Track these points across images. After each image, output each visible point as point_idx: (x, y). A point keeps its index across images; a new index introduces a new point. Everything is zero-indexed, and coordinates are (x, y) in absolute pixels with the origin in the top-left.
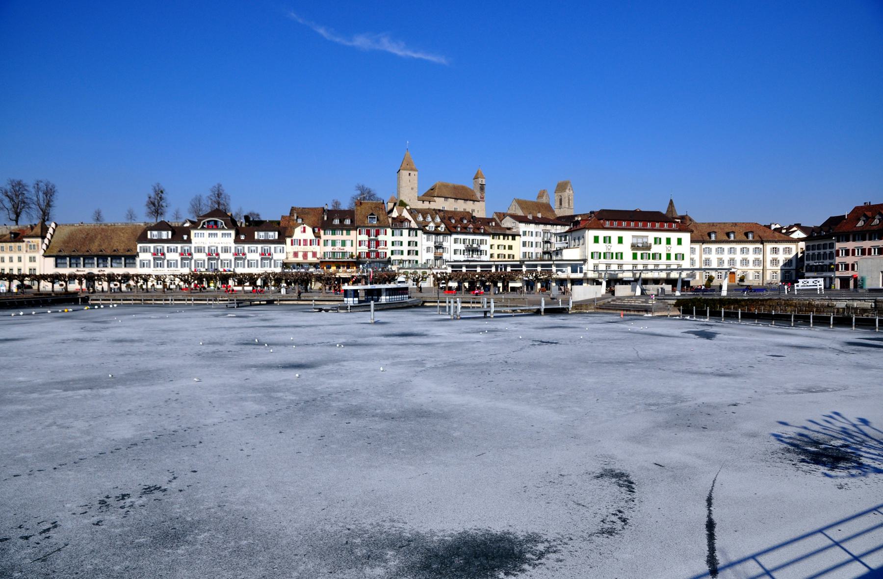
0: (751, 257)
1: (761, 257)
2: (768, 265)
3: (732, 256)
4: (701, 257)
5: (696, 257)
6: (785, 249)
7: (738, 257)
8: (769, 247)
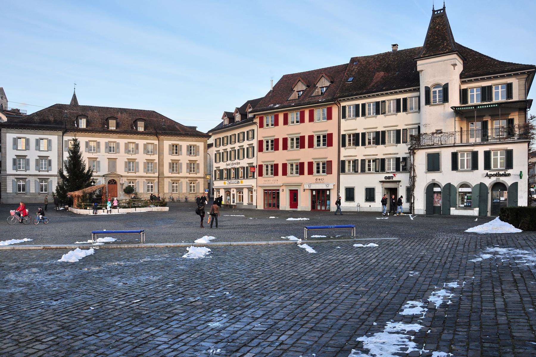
0: (141, 158)
2: (167, 172)
3: (112, 156)
6: (190, 148)
7: (122, 158)
8: (167, 143)
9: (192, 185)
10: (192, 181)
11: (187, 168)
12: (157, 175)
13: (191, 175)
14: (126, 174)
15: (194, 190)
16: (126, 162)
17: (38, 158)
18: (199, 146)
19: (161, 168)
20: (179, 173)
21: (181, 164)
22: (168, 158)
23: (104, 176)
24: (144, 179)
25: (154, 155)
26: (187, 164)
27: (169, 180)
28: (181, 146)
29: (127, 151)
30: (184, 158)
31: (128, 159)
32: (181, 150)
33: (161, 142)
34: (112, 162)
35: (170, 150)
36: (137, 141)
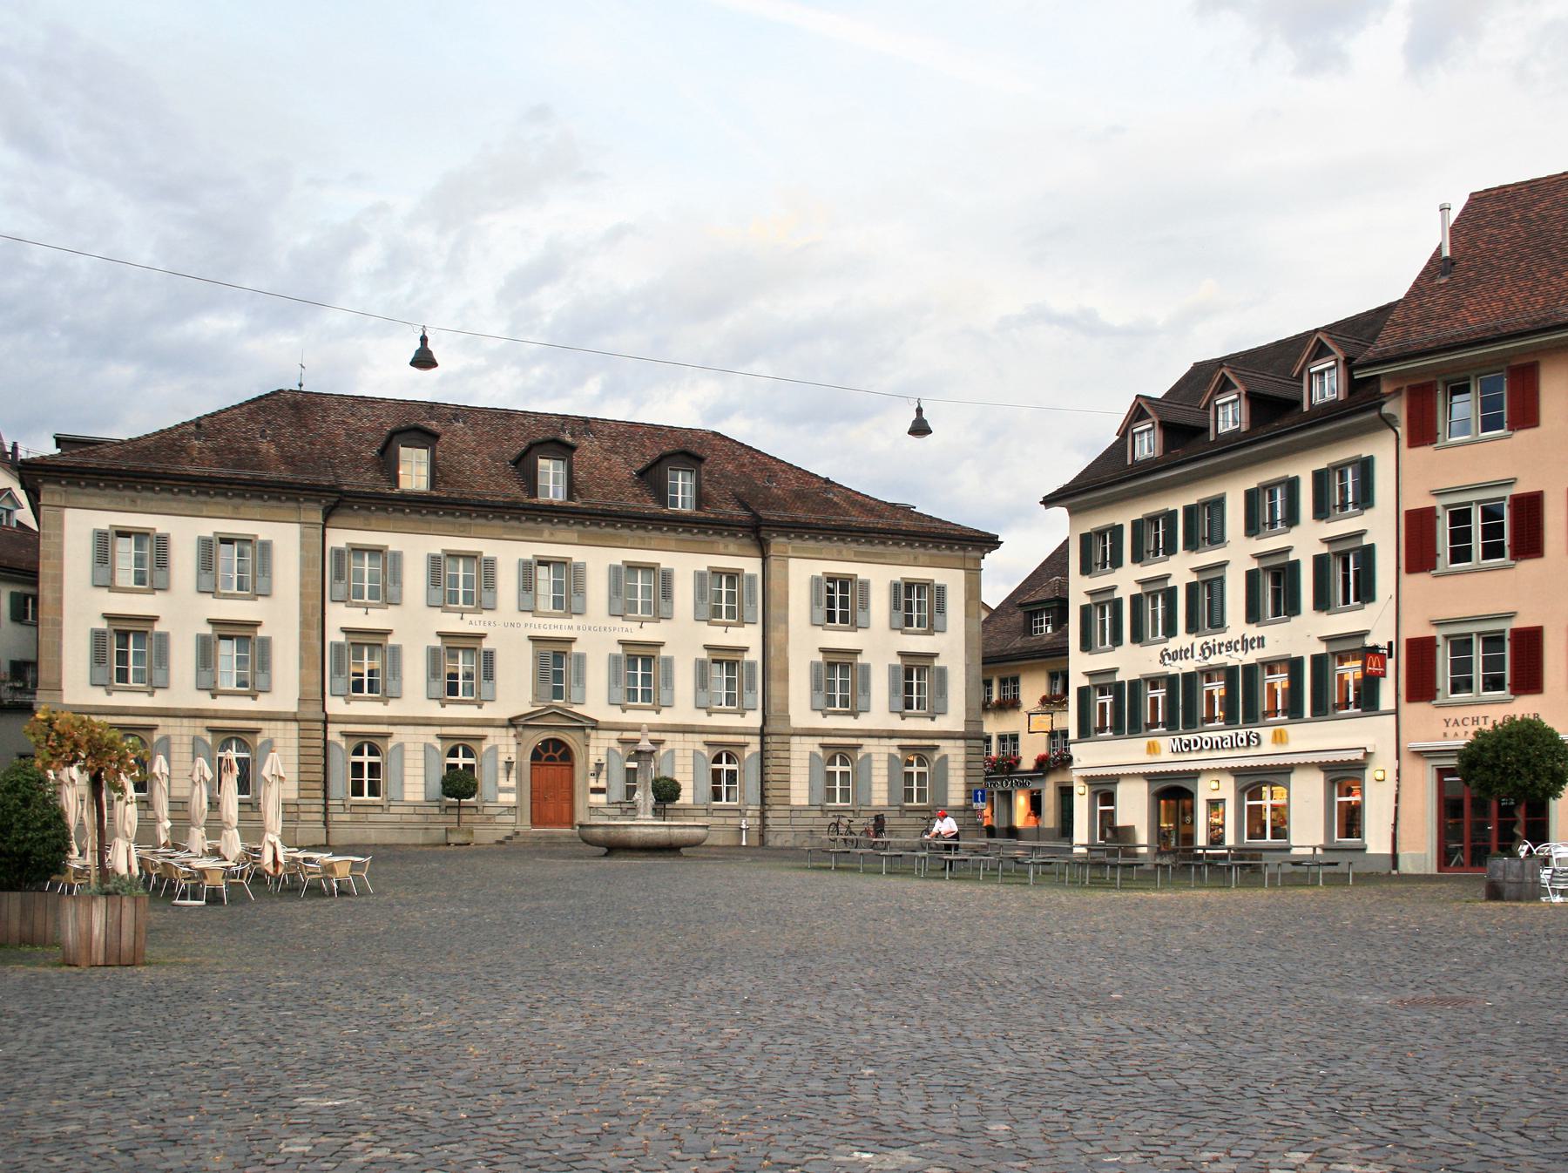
0: (684, 637)
1: (748, 637)
4: (314, 620)
5: (278, 616)
7: (597, 636)
8: (803, 572)
9: (915, 769)
10: (920, 751)
11: (893, 691)
12: (754, 720)
13: (912, 725)
14: (615, 715)
15: (921, 797)
16: (614, 659)
17: (208, 630)
18: (941, 590)
19: (775, 688)
20: (854, 714)
21: (866, 668)
22: (806, 641)
23: (512, 723)
24: (697, 741)
25: (741, 624)
26: (893, 668)
27: (812, 744)
28: (865, 585)
29: (621, 605)
30: (879, 643)
31: (623, 643)
32: (865, 605)
33: (774, 564)
34: (555, 660)
35: (815, 602)
36: (664, 559)
